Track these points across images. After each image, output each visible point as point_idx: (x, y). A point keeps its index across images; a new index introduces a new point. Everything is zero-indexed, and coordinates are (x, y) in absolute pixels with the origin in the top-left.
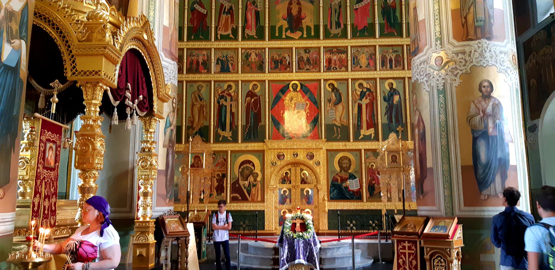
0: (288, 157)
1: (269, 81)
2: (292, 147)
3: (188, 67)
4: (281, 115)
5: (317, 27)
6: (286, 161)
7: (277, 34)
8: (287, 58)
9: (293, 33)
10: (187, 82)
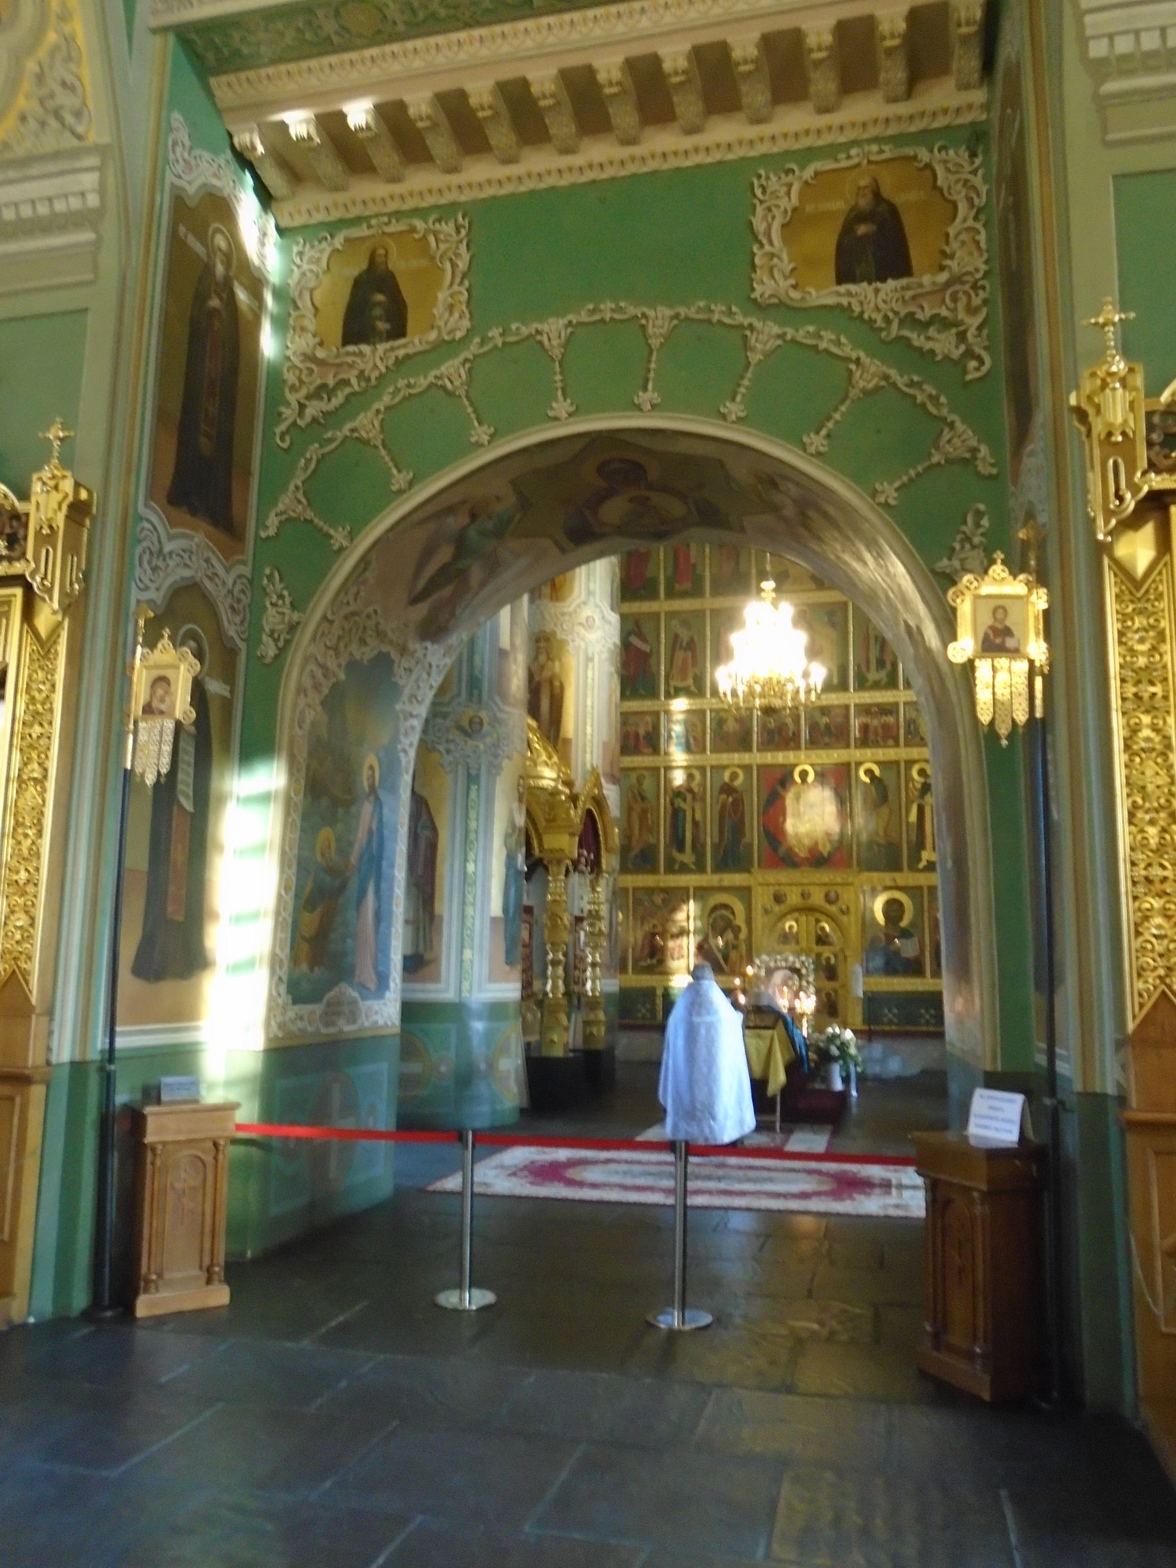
0: (794, 898)
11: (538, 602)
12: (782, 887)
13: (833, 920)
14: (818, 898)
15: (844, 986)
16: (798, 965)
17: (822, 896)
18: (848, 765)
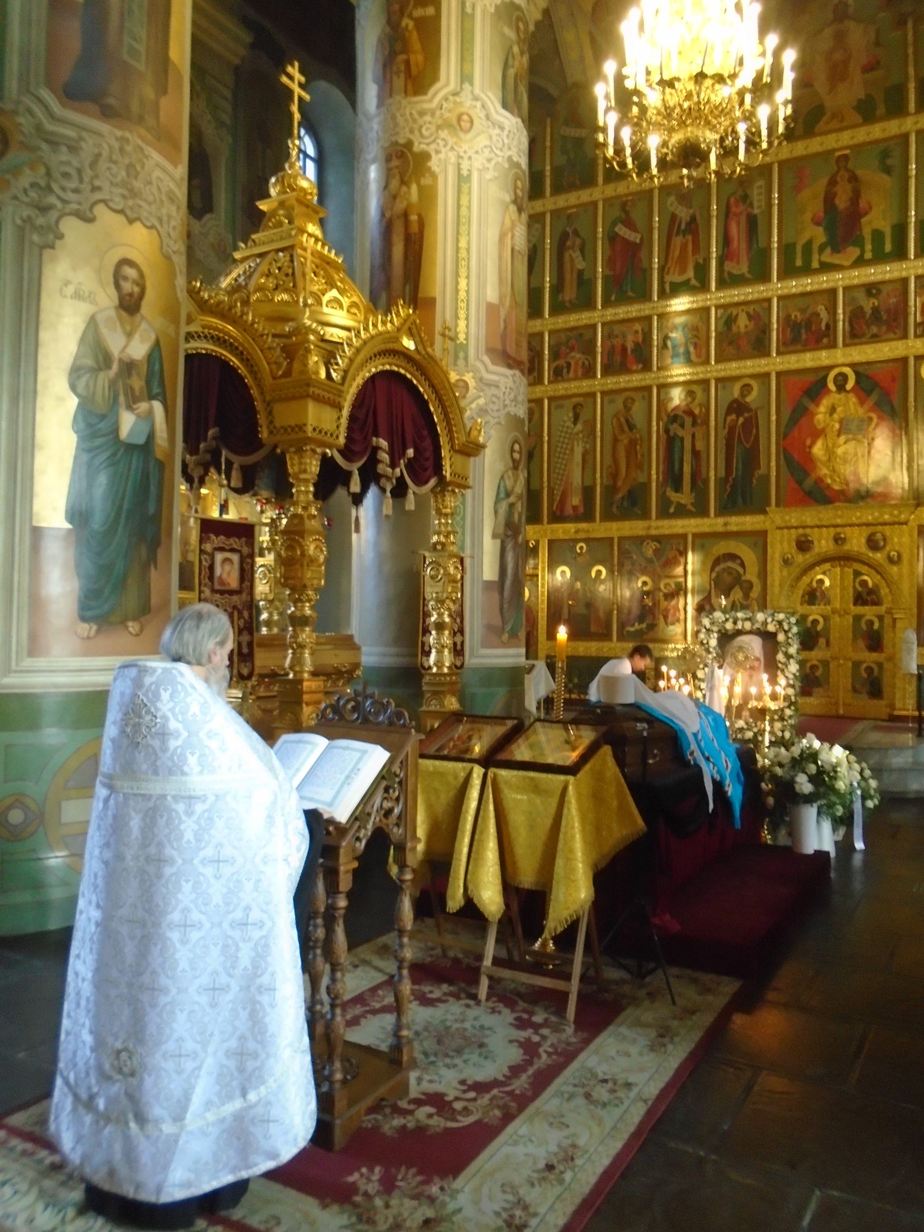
0: (823, 544)
1: (779, 374)
2: (834, 522)
3: (606, 361)
4: (808, 450)
5: (900, 231)
6: (818, 554)
7: (799, 263)
8: (824, 315)
9: (838, 252)
10: (603, 393)
11: (390, 101)
12: (808, 531)
13: (878, 572)
14: (857, 542)
15: (891, 659)
16: (771, 628)
17: (863, 541)
18: (905, 360)
